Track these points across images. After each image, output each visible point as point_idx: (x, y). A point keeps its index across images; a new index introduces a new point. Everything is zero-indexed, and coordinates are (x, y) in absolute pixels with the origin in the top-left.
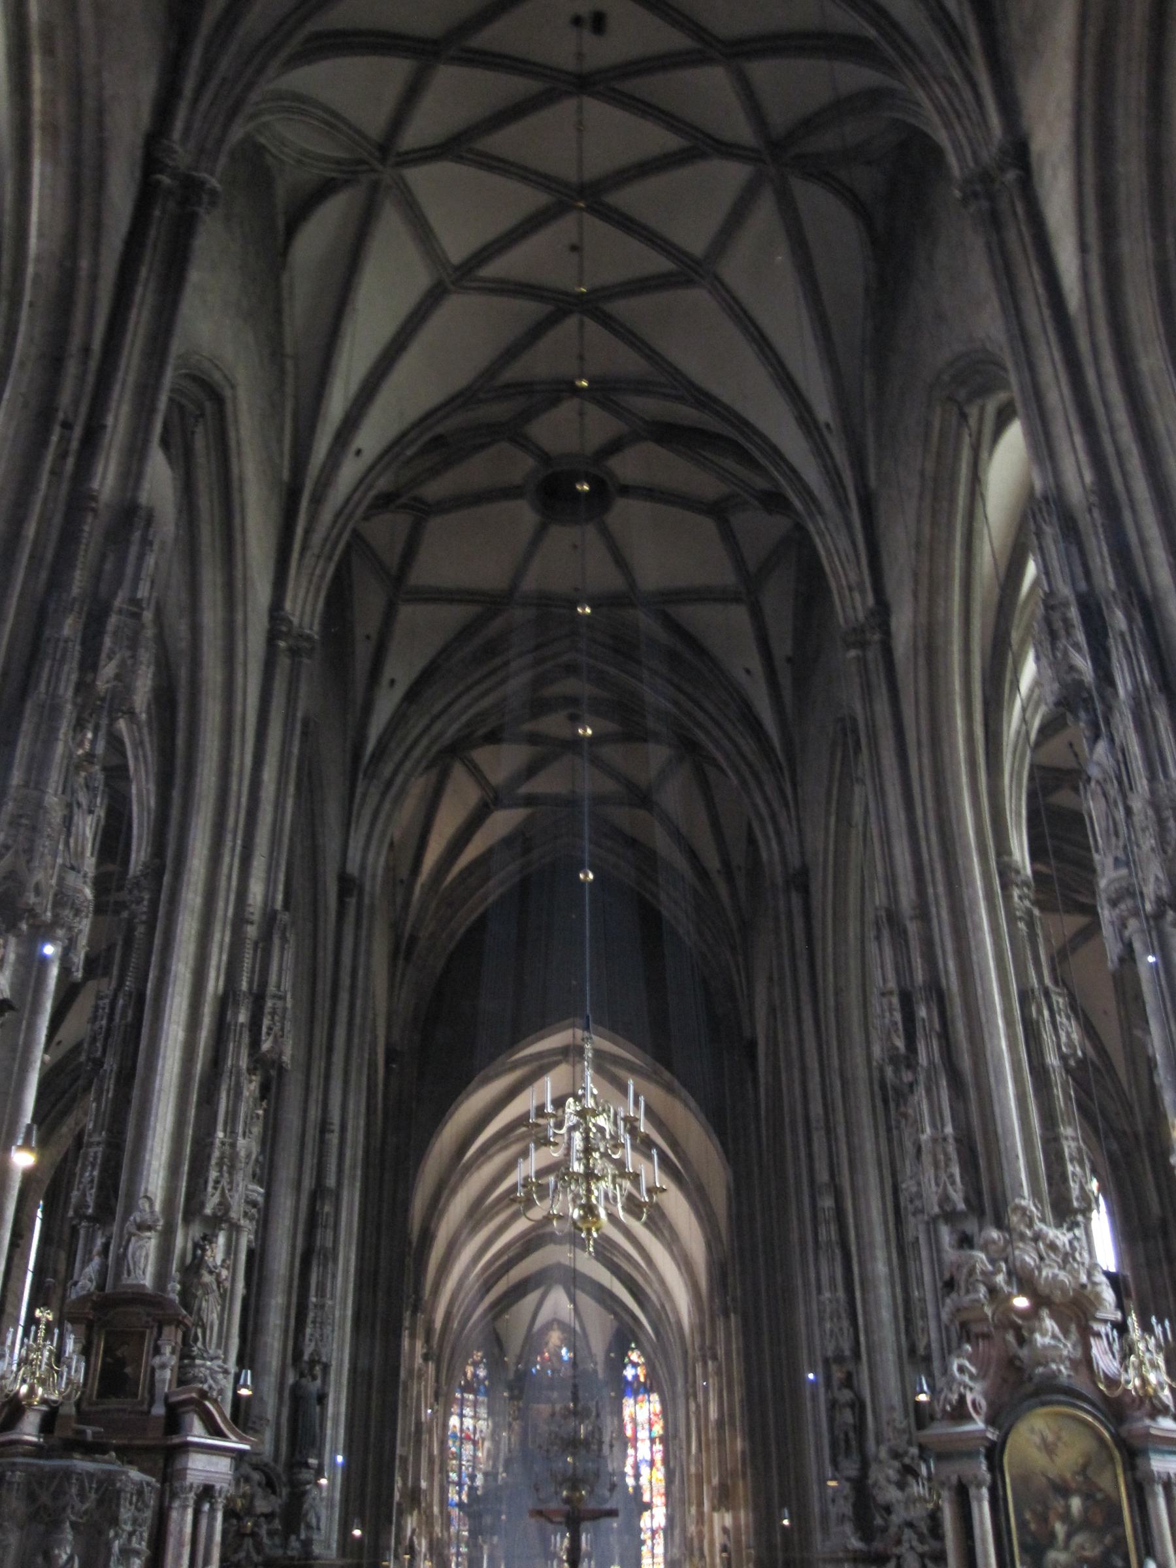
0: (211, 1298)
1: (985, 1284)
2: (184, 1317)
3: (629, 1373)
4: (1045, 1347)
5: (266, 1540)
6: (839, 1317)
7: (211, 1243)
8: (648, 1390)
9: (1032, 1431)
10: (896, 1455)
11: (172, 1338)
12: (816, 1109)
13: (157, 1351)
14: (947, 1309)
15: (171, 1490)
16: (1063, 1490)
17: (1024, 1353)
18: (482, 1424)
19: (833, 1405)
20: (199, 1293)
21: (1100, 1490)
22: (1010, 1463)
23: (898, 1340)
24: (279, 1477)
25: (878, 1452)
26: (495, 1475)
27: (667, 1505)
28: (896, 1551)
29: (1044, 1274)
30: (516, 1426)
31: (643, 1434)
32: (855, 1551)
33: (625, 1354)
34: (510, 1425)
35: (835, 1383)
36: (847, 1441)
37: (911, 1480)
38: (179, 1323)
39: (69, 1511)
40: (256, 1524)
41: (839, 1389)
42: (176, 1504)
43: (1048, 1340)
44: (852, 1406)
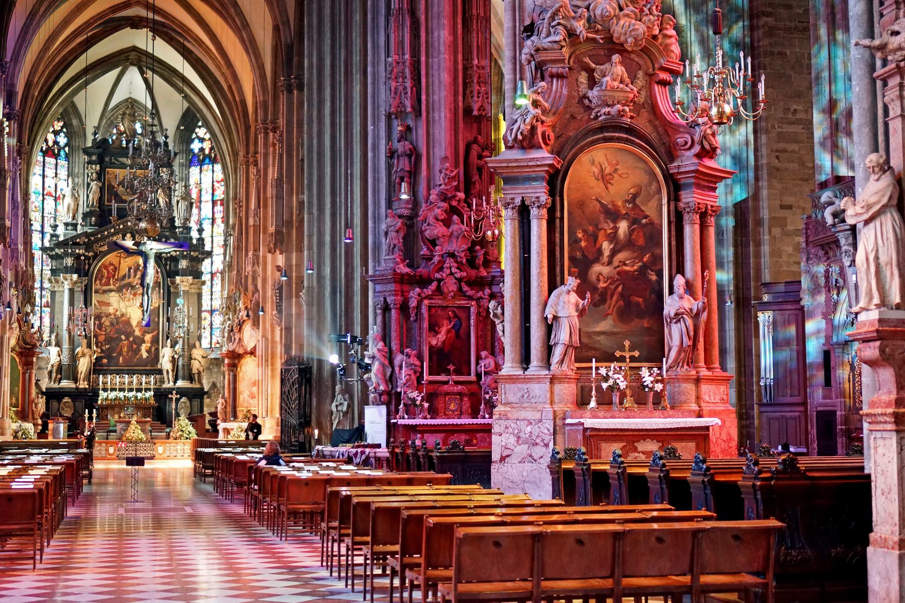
1: (565, 27)
3: (196, 146)
4: (613, 89)
6: (404, 78)
8: (214, 161)
9: (593, 163)
10: (444, 197)
14: (525, 50)
16: (614, 215)
17: (594, 94)
18: (62, 184)
19: (391, 154)
21: (646, 217)
22: (569, 188)
23: (456, 101)
25: (430, 195)
26: (75, 226)
27: (225, 254)
28: (437, 276)
29: (622, 22)
30: (94, 185)
31: (206, 197)
32: (402, 275)
33: (193, 131)
34: (88, 184)
35: (396, 135)
37: (455, 218)
41: (399, 141)
43: (616, 84)
44: (410, 156)
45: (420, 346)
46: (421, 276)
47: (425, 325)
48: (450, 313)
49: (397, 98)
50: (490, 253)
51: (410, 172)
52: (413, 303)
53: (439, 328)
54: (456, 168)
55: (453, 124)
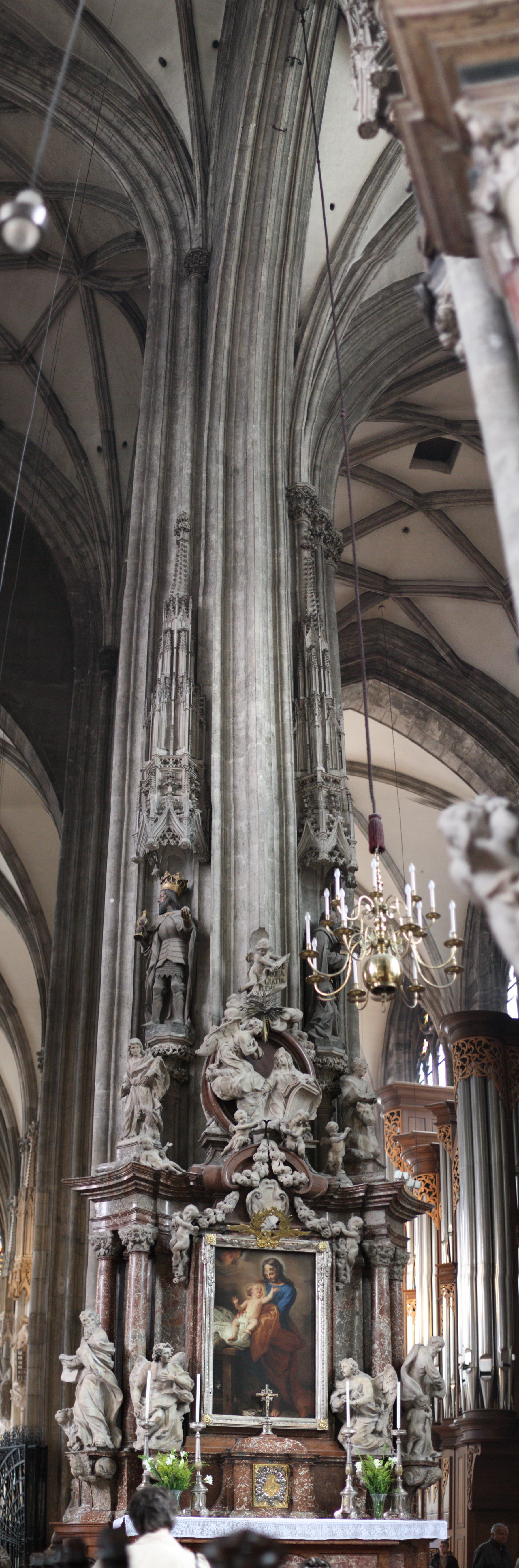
12: (181, 507)
19: (146, 936)
32: (157, 1174)
36: (167, 995)
37: (283, 1055)
41: (163, 911)
44: (183, 936)
45: (194, 1342)
46: (199, 1179)
47: (208, 1290)
48: (268, 1267)
49: (162, 819)
50: (360, 1143)
51: (184, 967)
52: (180, 1240)
53: (241, 1302)
54: (283, 954)
55: (277, 877)
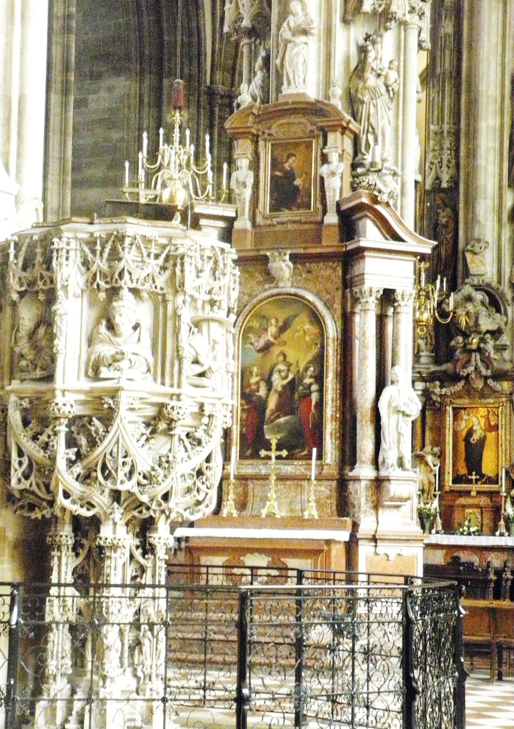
0: (379, 101)
2: (349, 122)
5: (492, 355)
7: (374, 43)
11: (339, 144)
13: (325, 159)
15: (352, 296)
20: (366, 99)
24: (503, 295)
38: (344, 129)
39: (126, 276)
40: (483, 340)
42: (358, 309)
